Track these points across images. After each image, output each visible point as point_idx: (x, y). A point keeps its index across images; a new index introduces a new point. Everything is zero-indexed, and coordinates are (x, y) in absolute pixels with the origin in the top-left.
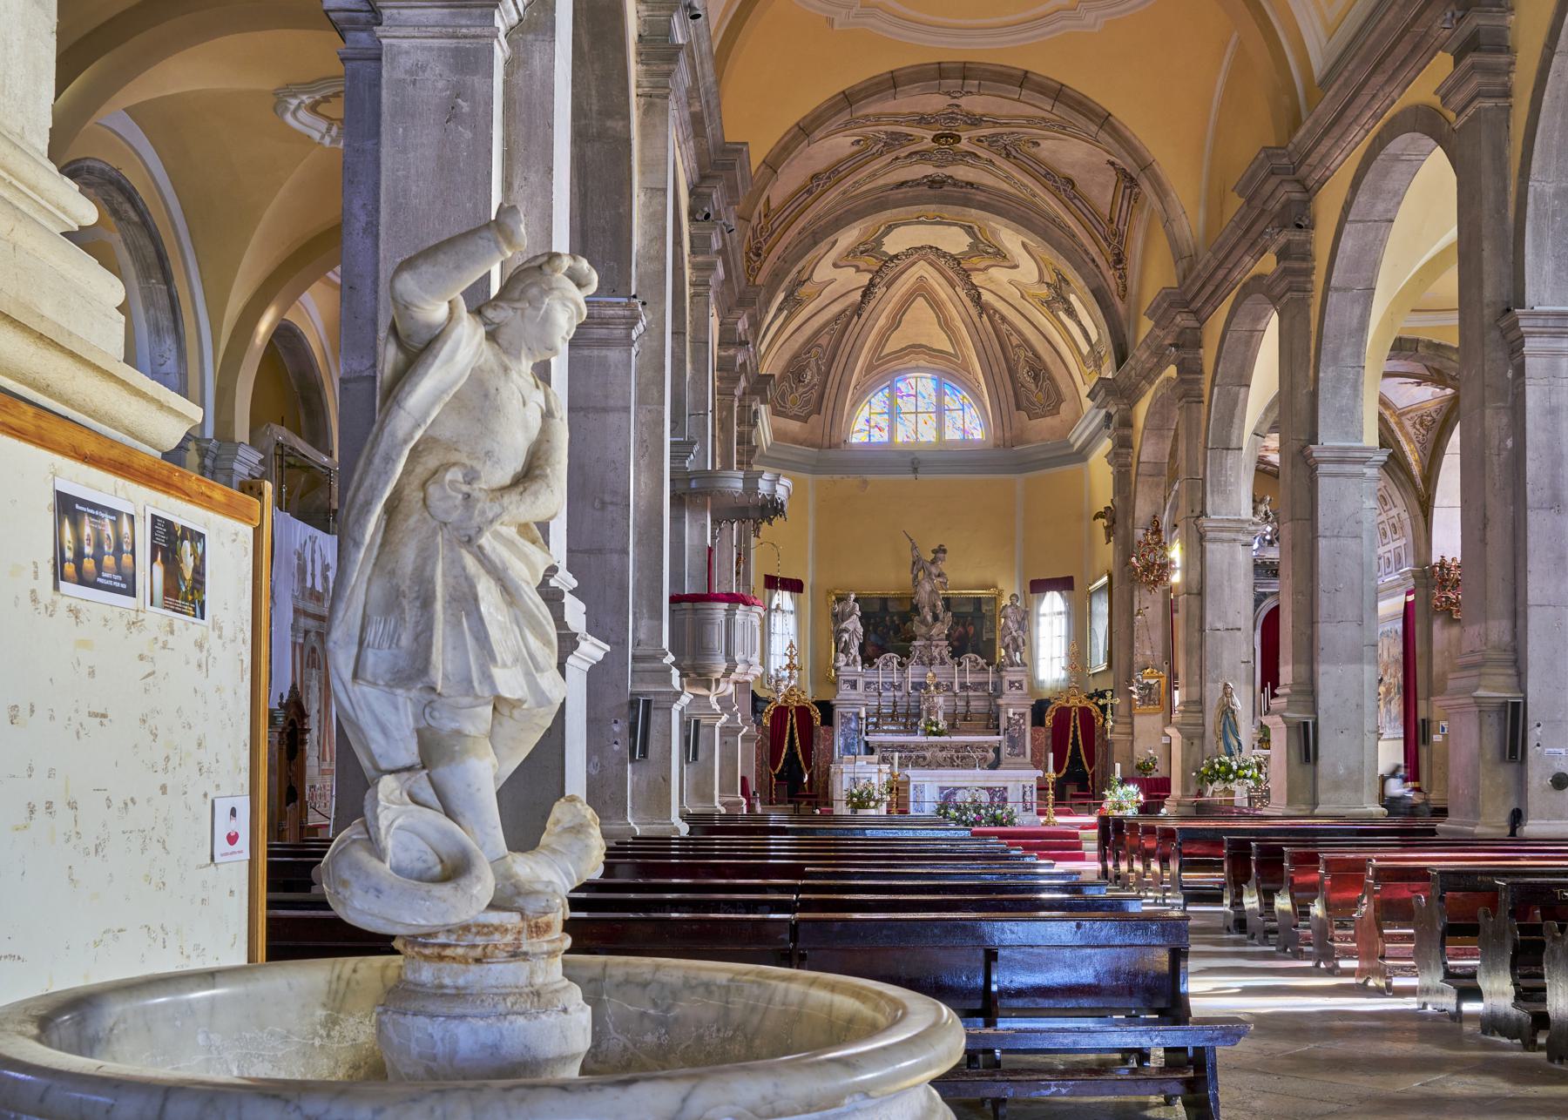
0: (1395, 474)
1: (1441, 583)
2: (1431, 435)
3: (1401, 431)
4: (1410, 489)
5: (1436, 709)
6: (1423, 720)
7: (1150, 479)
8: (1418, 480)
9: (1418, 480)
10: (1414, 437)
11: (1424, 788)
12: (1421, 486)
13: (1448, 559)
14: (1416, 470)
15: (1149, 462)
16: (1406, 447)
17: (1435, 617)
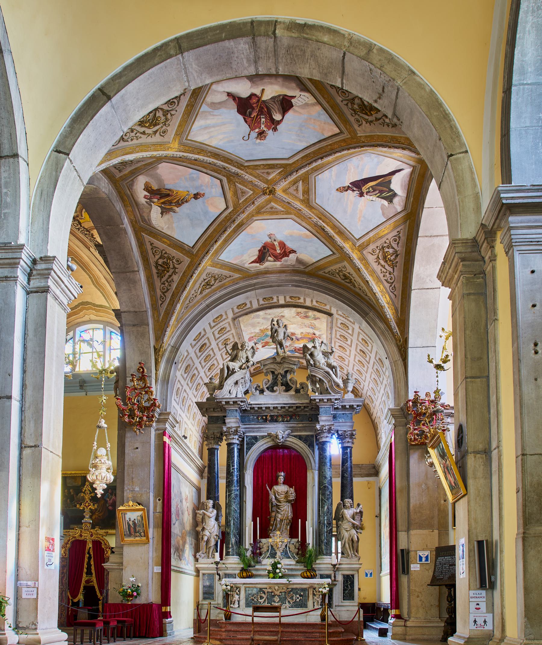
0: (375, 324)
1: (415, 418)
2: (398, 273)
3: (367, 269)
4: (389, 336)
5: (413, 539)
6: (402, 551)
7: (134, 329)
8: (393, 324)
9: (393, 324)
10: (381, 276)
11: (405, 615)
12: (396, 329)
13: (422, 396)
14: (389, 313)
15: (129, 312)
16: (376, 288)
17: (411, 451)
